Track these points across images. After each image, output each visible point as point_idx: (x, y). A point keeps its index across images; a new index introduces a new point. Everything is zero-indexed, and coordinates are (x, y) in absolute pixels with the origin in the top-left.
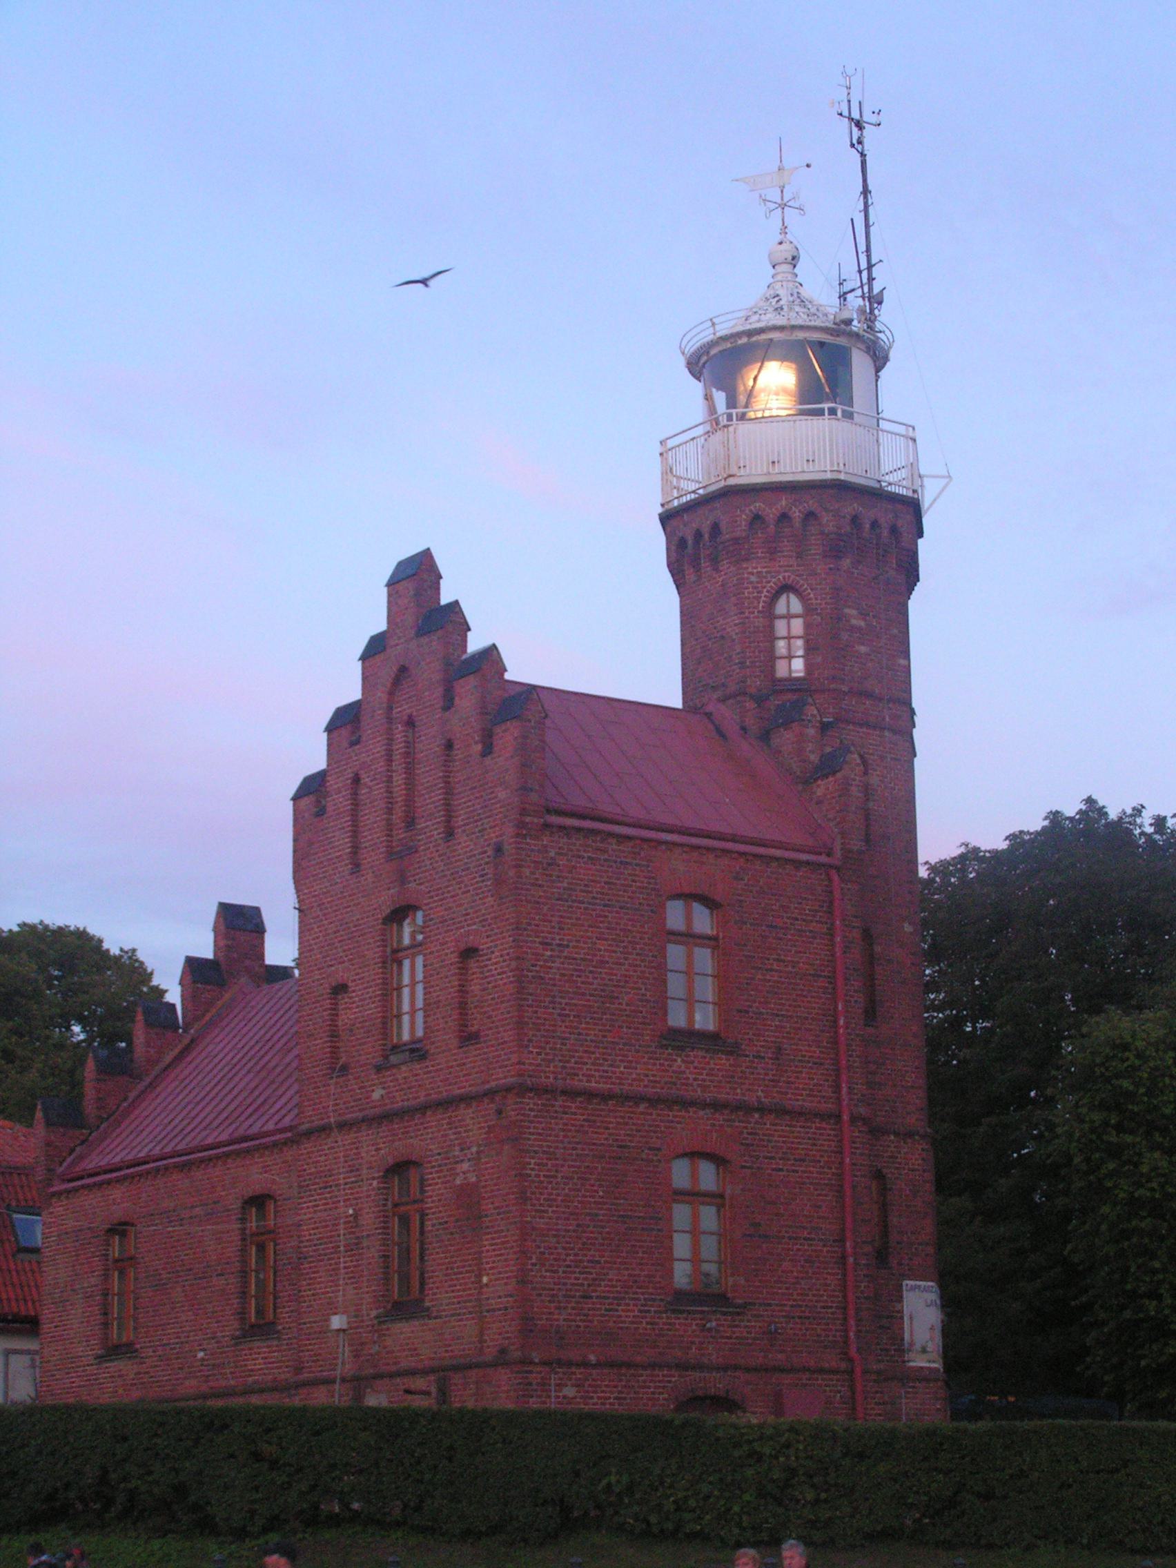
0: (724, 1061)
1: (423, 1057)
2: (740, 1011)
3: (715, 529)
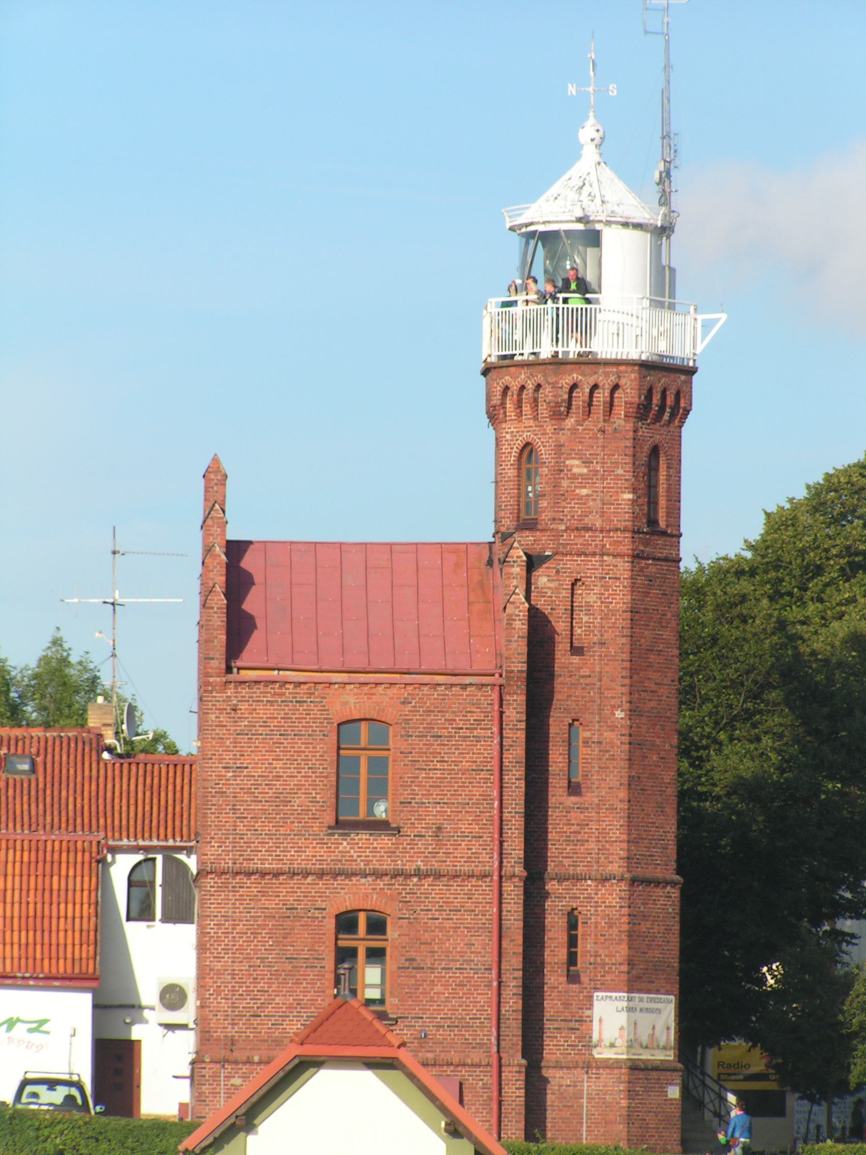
0: (385, 841)
2: (401, 803)
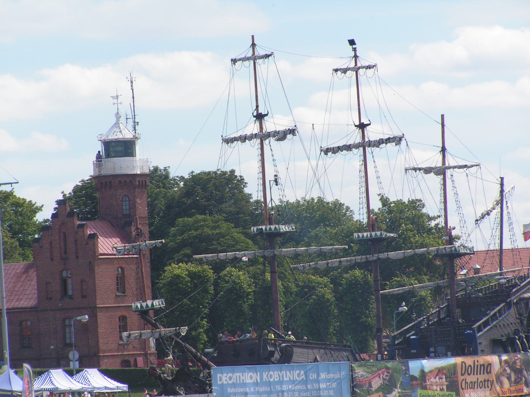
1: (72, 299)
3: (110, 182)
